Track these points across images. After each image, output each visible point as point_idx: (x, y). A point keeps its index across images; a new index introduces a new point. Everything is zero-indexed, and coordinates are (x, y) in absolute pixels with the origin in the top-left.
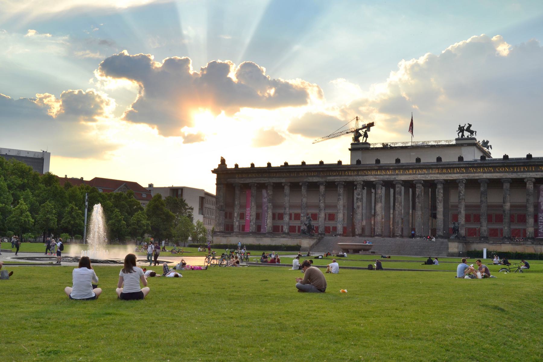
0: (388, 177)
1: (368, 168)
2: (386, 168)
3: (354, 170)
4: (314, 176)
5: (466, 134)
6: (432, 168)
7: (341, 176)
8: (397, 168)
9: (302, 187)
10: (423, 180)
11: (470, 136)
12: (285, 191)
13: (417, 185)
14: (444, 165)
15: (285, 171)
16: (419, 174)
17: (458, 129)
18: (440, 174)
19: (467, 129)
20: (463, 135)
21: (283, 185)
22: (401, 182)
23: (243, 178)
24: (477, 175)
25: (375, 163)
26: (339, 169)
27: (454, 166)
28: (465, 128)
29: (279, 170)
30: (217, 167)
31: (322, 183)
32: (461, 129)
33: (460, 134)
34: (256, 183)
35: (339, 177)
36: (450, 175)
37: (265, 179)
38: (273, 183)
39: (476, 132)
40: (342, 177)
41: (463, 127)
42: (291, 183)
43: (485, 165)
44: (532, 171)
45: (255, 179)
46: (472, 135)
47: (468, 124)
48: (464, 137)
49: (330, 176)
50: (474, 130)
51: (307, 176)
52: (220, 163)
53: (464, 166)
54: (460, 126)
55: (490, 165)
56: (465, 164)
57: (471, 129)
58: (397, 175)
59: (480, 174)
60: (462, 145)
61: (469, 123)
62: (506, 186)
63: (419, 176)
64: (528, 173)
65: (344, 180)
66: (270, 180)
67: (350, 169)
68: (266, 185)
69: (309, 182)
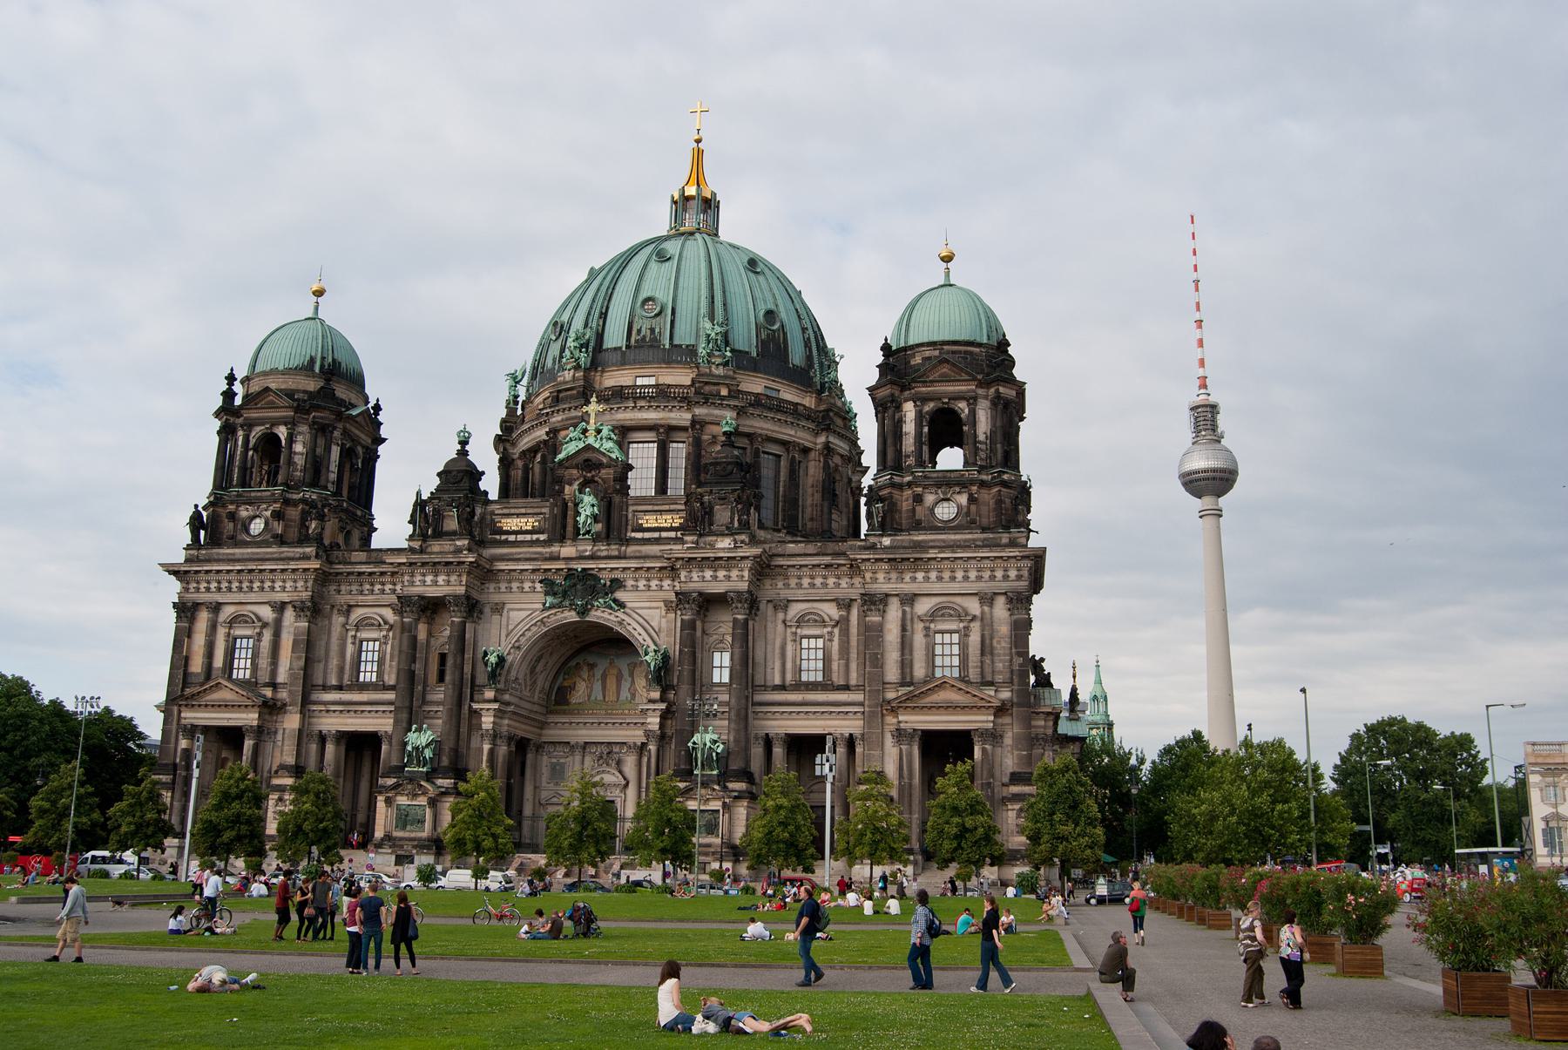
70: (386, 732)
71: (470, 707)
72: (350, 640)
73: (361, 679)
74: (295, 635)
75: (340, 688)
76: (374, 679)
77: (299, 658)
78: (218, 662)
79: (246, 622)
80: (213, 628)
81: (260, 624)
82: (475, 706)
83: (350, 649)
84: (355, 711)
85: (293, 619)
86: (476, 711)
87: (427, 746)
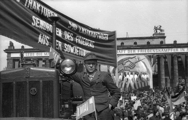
5: (159, 31)
11: (160, 33)
17: (154, 29)
19: (159, 28)
20: (157, 32)
28: (158, 28)
30: (7, 48)
32: (156, 29)
33: (155, 31)
39: (164, 30)
41: (157, 27)
46: (162, 32)
47: (160, 26)
48: (157, 33)
50: (163, 29)
52: (9, 45)
54: (155, 27)
57: (162, 28)
61: (161, 25)
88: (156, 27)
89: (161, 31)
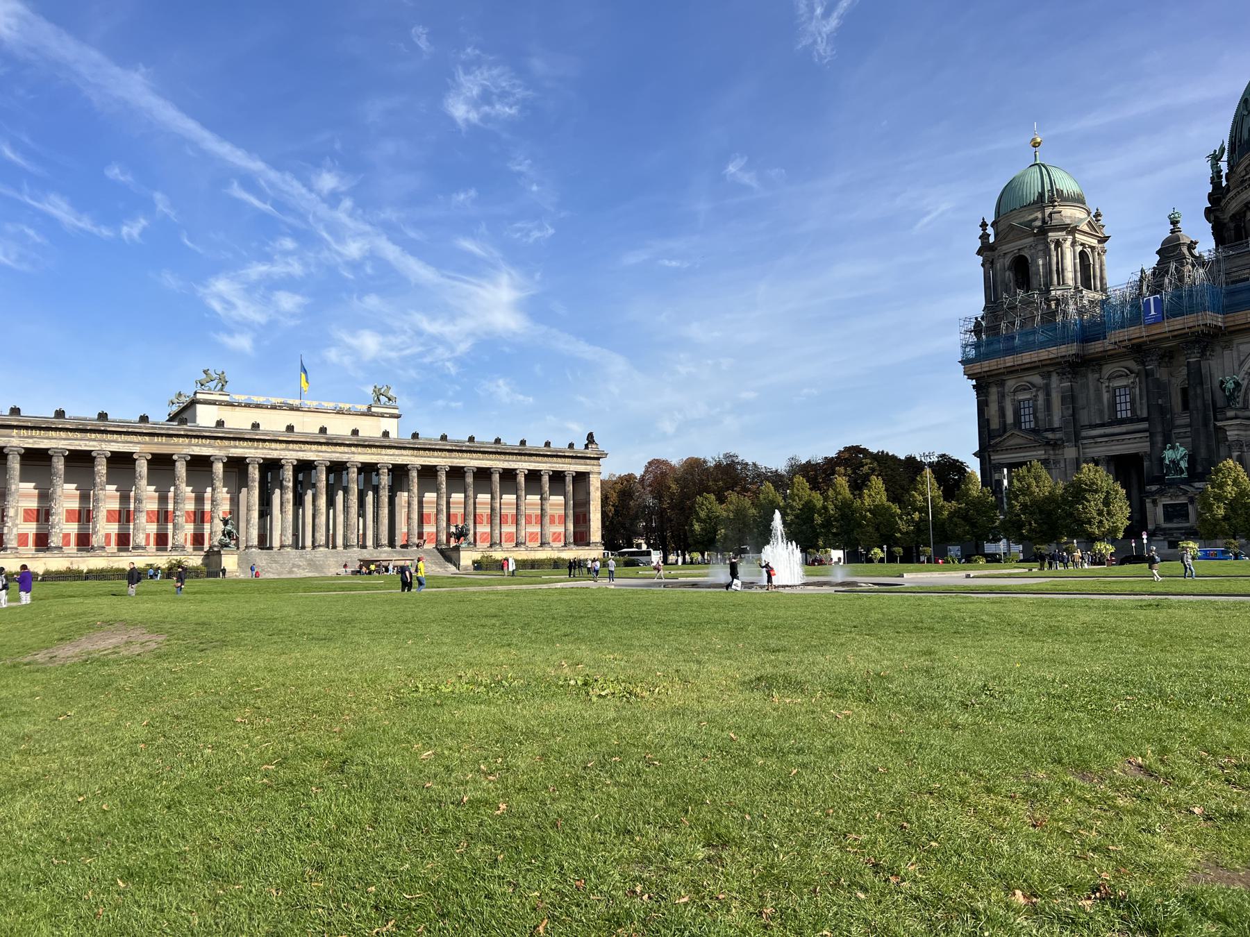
0: (338, 455)
1: (308, 440)
2: (339, 441)
3: (281, 442)
4: (204, 446)
5: (383, 399)
6: (405, 448)
7: (256, 448)
8: (356, 443)
9: (178, 464)
10: (392, 464)
12: (138, 469)
13: (381, 471)
14: (424, 444)
15: (145, 431)
16: (386, 455)
18: (416, 456)
21: (135, 456)
22: (360, 465)
23: (32, 437)
24: (462, 461)
25: (53, 416)
26: (257, 437)
27: (437, 447)
29: (130, 430)
31: (220, 459)
34: (68, 450)
35: (253, 451)
36: (429, 459)
37: (92, 443)
38: (111, 452)
40: (259, 451)
41: (380, 390)
42: (151, 454)
43: (475, 449)
44: (525, 462)
45: (63, 442)
49: (236, 447)
51: (190, 445)
53: (450, 448)
55: (482, 449)
56: (451, 445)
57: (391, 393)
58: (353, 453)
59: (466, 461)
60: (382, 415)
62: (496, 477)
63: (386, 457)
64: (520, 463)
65: (263, 456)
66: (103, 446)
67: (277, 438)
68: (94, 454)
69: (190, 455)
70: (1145, 452)
71: (1215, 425)
72: (1104, 390)
73: (1119, 417)
74: (1062, 393)
75: (1103, 425)
76: (1129, 415)
77: (1068, 408)
78: (1010, 419)
79: (1025, 390)
80: (1002, 396)
81: (1035, 389)
82: (1219, 424)
83: (1106, 396)
84: (1118, 440)
85: (1058, 382)
86: (1220, 428)
87: (1182, 458)
88: (378, 387)
89: (390, 399)
